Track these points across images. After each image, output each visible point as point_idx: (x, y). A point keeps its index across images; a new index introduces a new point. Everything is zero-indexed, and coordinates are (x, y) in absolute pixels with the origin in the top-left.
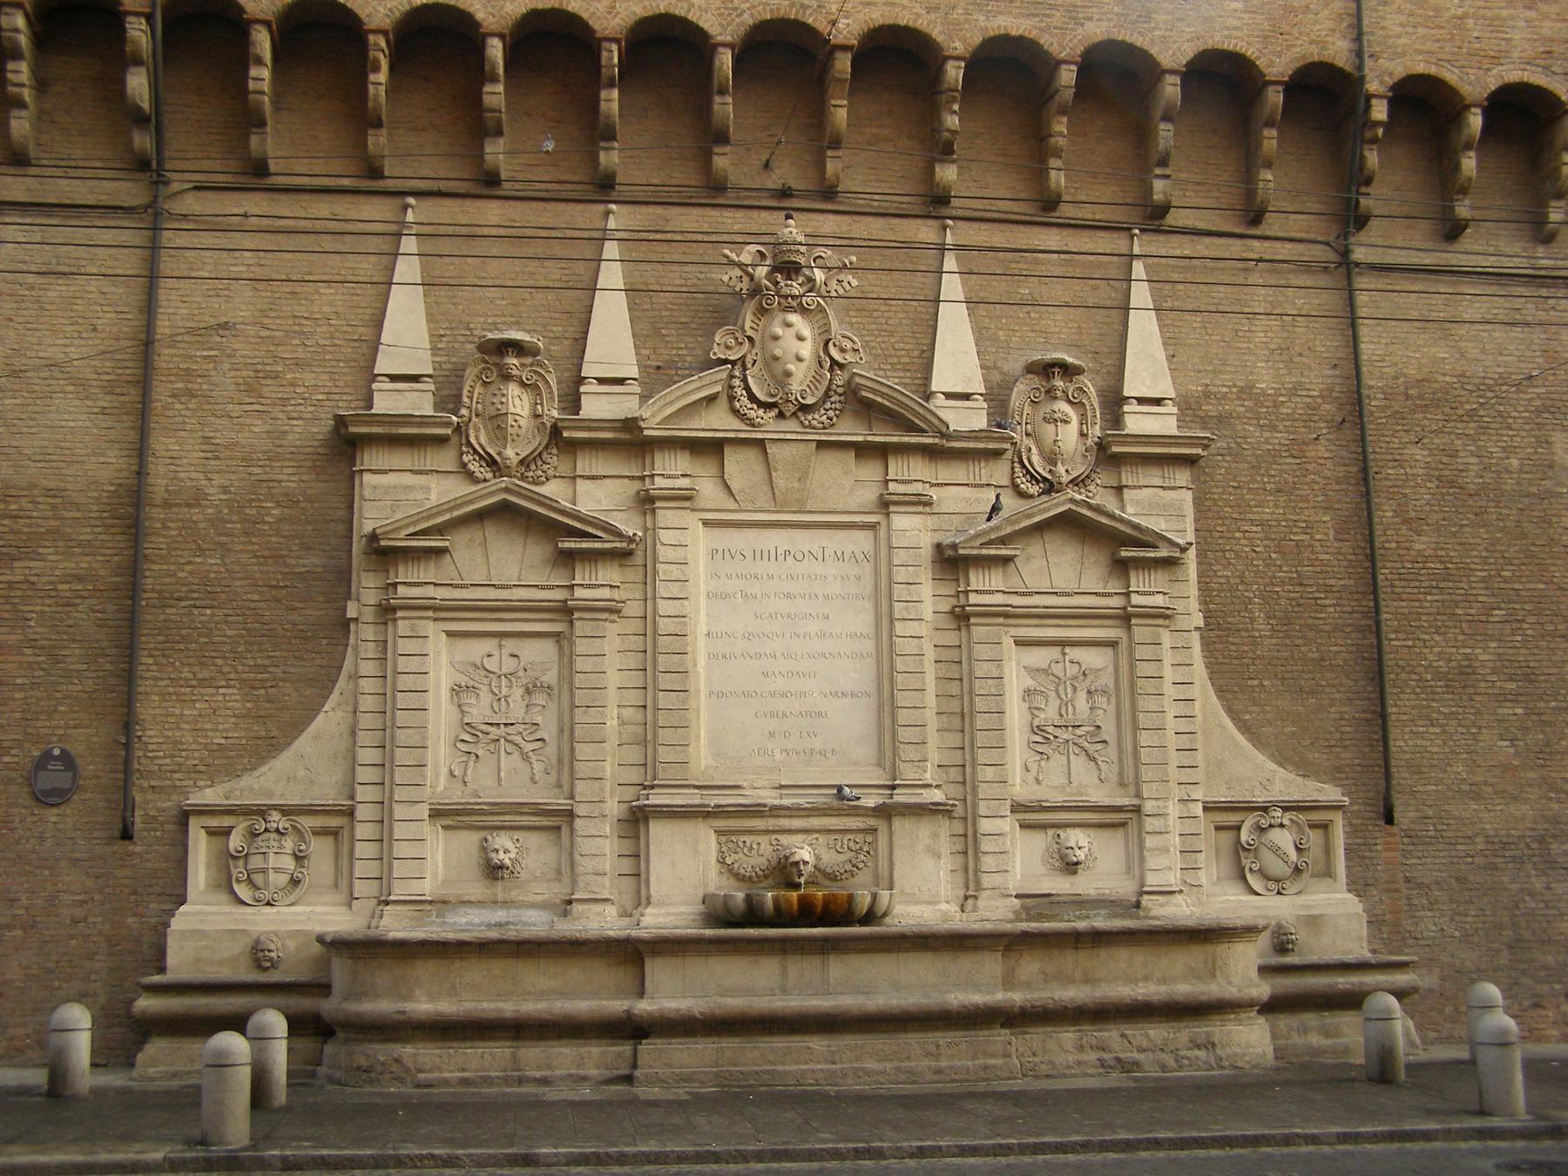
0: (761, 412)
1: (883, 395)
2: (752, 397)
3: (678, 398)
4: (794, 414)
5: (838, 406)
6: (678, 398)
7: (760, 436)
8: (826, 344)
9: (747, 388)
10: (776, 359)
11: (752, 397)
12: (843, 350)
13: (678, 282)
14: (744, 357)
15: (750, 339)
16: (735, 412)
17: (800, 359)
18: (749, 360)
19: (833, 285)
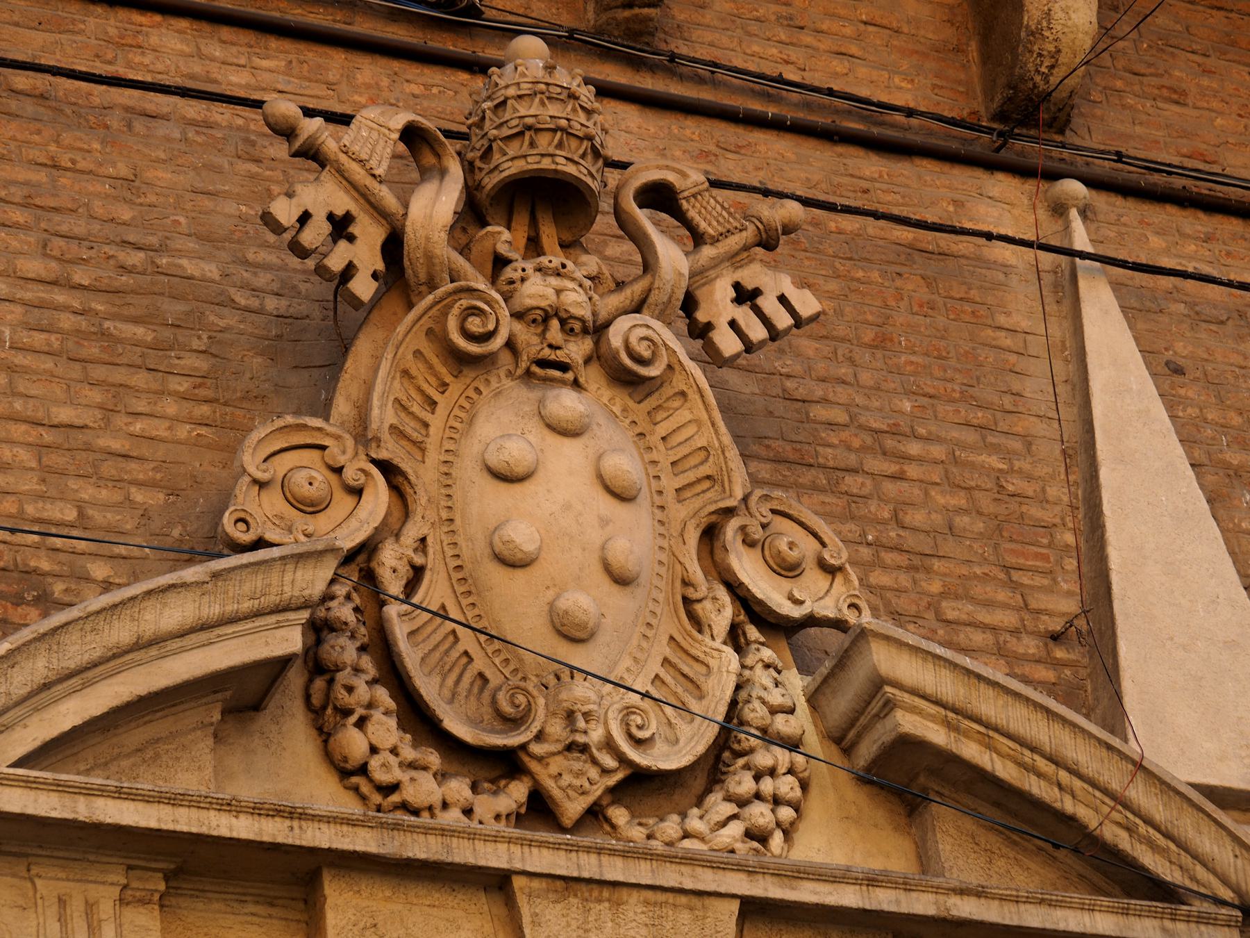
0: (459, 788)
1: (990, 729)
2: (418, 717)
3: (116, 659)
4: (595, 815)
5: (787, 786)
6: (116, 659)
7: (495, 857)
8: (710, 534)
9: (394, 675)
10: (512, 562)
11: (418, 717)
12: (787, 569)
13: (33, 266)
14: (367, 549)
15: (388, 469)
16: (349, 773)
17: (622, 580)
18: (391, 562)
19: (719, 304)
